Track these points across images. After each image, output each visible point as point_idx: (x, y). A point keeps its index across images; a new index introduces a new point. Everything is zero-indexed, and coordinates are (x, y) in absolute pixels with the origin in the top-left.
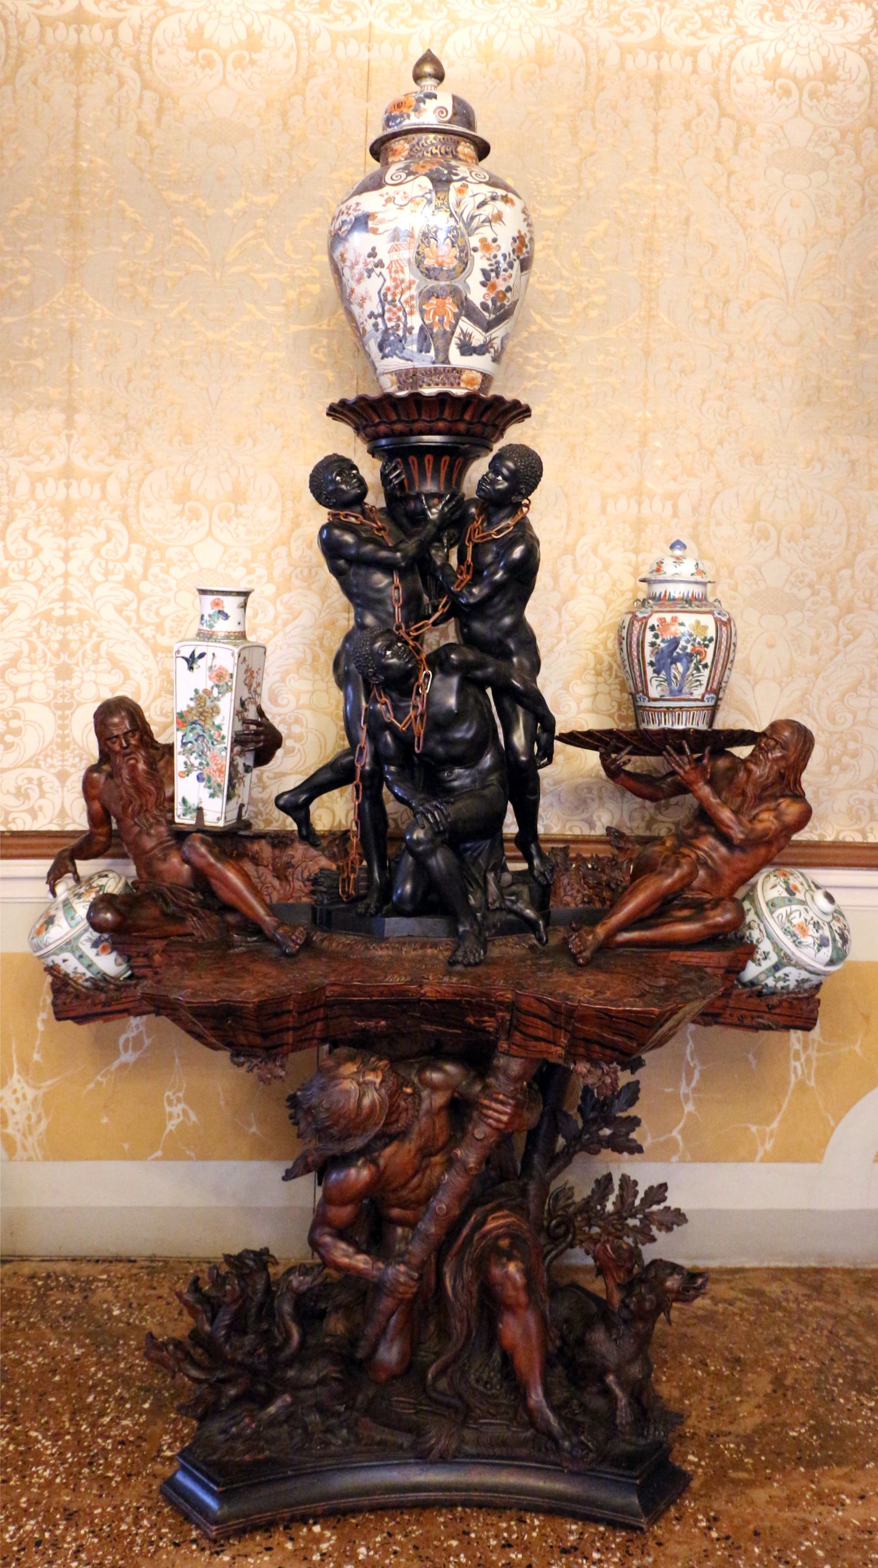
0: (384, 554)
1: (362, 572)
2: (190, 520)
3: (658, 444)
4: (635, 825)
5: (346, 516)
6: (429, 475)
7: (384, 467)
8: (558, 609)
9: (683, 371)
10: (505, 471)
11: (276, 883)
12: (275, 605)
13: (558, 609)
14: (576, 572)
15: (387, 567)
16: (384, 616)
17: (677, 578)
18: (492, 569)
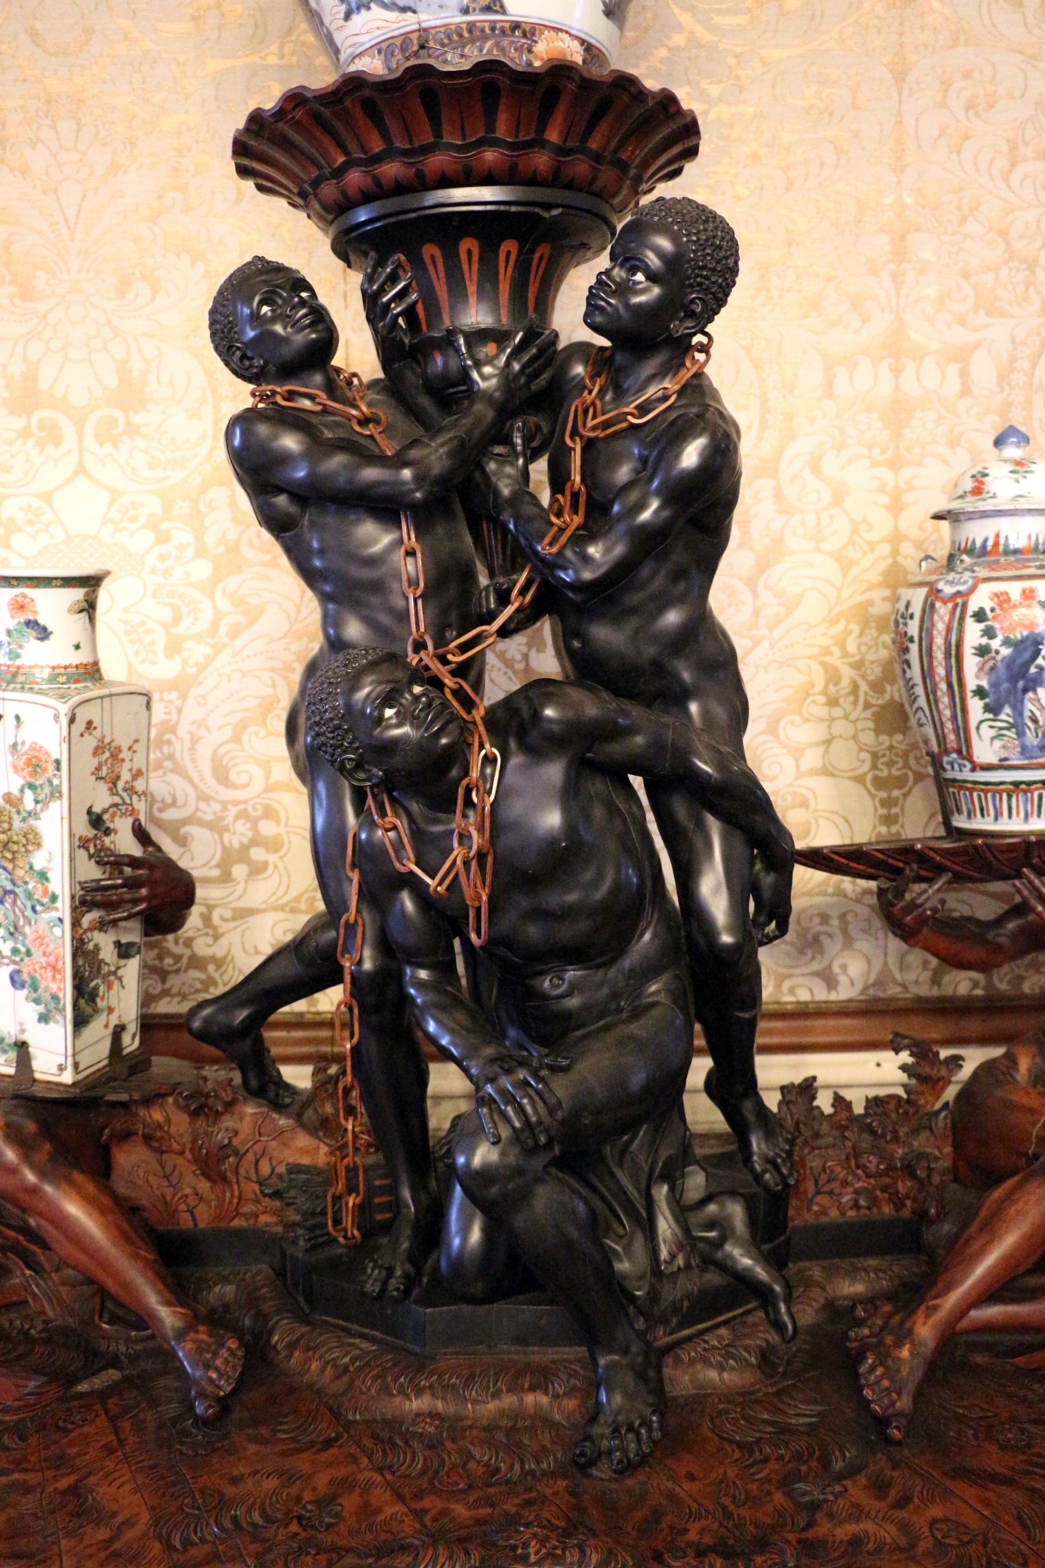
0: (371, 474)
1: (330, 520)
2: (41, 444)
3: (927, 255)
4: (911, 976)
5: (291, 396)
6: (472, 288)
7: (370, 279)
8: (751, 584)
9: (970, 106)
10: (653, 260)
11: (204, 1186)
12: (212, 598)
13: (751, 584)
14: (780, 512)
15: (385, 507)
16: (384, 619)
17: (1023, 504)
18: (634, 496)
